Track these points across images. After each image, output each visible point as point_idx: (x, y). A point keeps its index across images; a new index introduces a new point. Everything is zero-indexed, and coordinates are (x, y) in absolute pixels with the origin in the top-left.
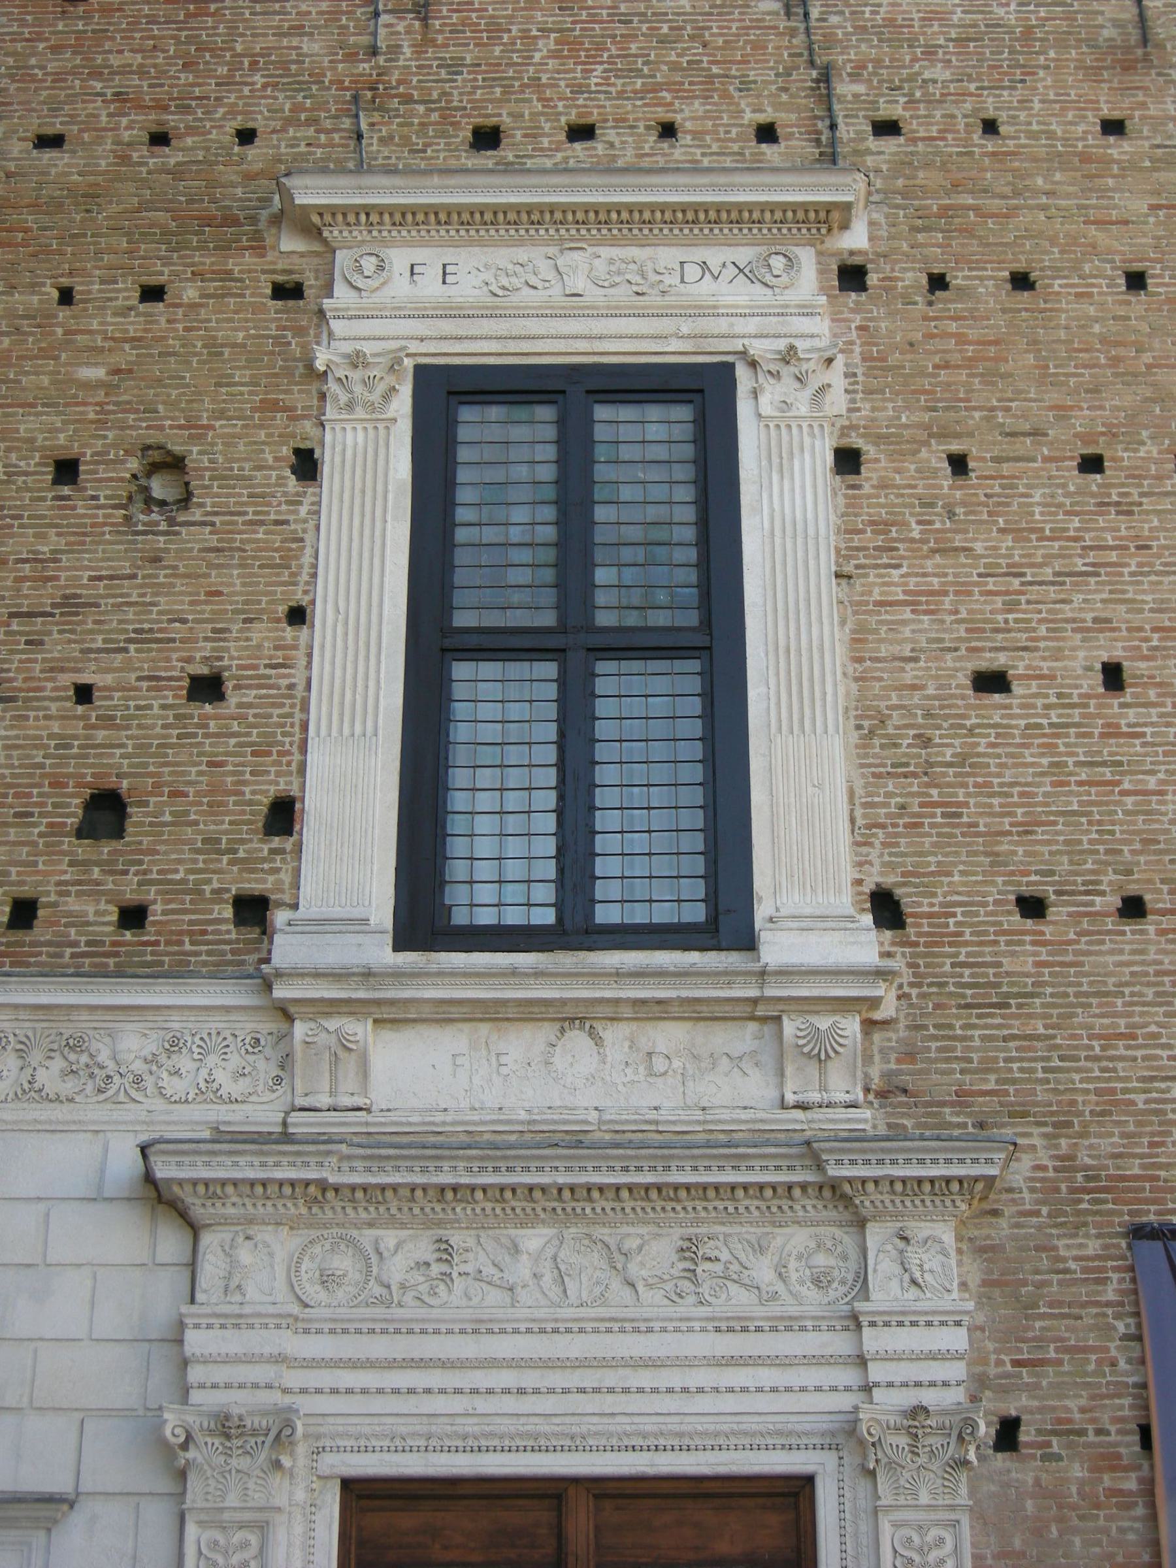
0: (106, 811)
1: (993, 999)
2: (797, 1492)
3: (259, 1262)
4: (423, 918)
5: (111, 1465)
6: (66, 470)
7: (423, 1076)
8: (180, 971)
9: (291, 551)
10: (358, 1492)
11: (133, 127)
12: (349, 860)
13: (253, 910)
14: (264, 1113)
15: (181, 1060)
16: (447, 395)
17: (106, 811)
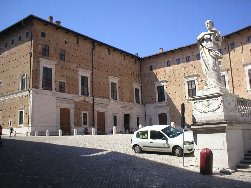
0: (152, 99)
1: (170, 102)
2: (166, 113)
3: (156, 110)
4: (159, 101)
5: (154, 114)
6: (150, 91)
7: (159, 105)
8: (154, 103)
9: (155, 92)
10: (159, 114)
11: (150, 80)
12: (157, 100)
13: (155, 101)
14: (156, 106)
15: (154, 105)
16: (158, 87)
17: (152, 99)
